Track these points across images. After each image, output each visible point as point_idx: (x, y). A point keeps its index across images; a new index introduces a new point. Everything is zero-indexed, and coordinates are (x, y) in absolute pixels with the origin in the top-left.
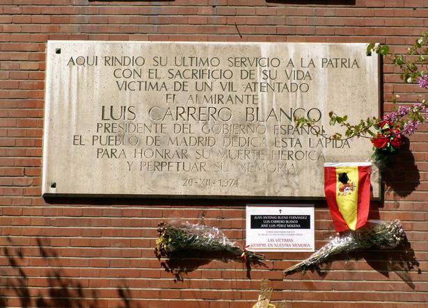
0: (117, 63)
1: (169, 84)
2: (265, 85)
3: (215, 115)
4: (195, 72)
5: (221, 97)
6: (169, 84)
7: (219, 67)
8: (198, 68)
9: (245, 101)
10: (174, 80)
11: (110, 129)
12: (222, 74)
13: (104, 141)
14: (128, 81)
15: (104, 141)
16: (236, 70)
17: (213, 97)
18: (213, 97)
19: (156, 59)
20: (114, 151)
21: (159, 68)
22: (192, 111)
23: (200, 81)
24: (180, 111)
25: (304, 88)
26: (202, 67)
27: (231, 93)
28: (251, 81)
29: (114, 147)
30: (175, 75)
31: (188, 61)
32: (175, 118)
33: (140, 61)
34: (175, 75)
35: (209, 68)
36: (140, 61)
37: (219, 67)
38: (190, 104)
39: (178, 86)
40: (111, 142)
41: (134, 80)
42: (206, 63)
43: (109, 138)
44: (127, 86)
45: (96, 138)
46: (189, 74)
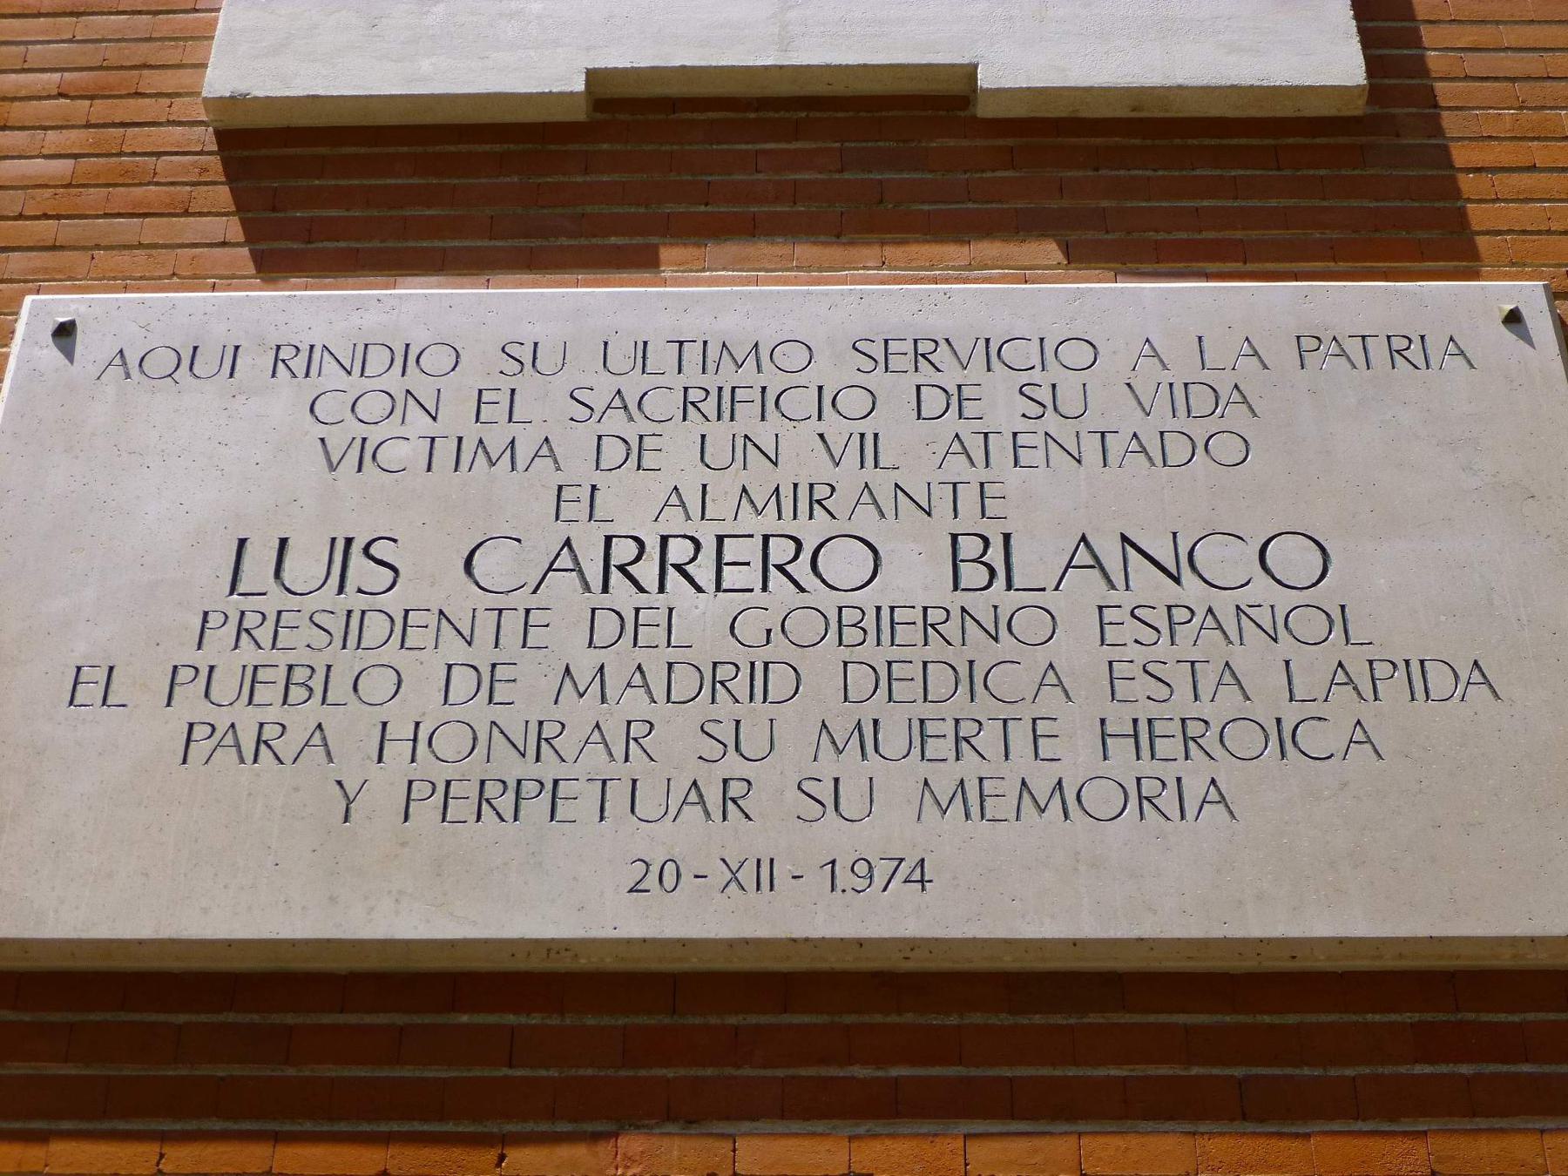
0: (330, 365)
1: (575, 445)
2: (1038, 440)
3: (801, 569)
4: (695, 395)
5: (821, 492)
6: (575, 445)
7: (812, 377)
8: (710, 382)
9: (943, 506)
10: (594, 428)
11: (266, 635)
12: (825, 402)
13: (225, 687)
14: (375, 435)
15: (225, 687)
16: (896, 388)
17: (787, 492)
18: (787, 492)
19: (513, 350)
20: (270, 732)
21: (527, 384)
22: (679, 551)
23: (720, 434)
24: (623, 551)
25: (1227, 449)
26: (728, 376)
27: (869, 473)
28: (964, 428)
29: (274, 713)
30: (599, 407)
31: (662, 356)
32: (596, 581)
33: (438, 360)
34: (599, 407)
35: (762, 380)
36: (438, 360)
37: (812, 377)
38: (673, 522)
39: (613, 452)
40: (262, 694)
41: (401, 432)
42: (751, 361)
43: (253, 678)
44: (367, 455)
45: (185, 675)
46: (664, 404)
